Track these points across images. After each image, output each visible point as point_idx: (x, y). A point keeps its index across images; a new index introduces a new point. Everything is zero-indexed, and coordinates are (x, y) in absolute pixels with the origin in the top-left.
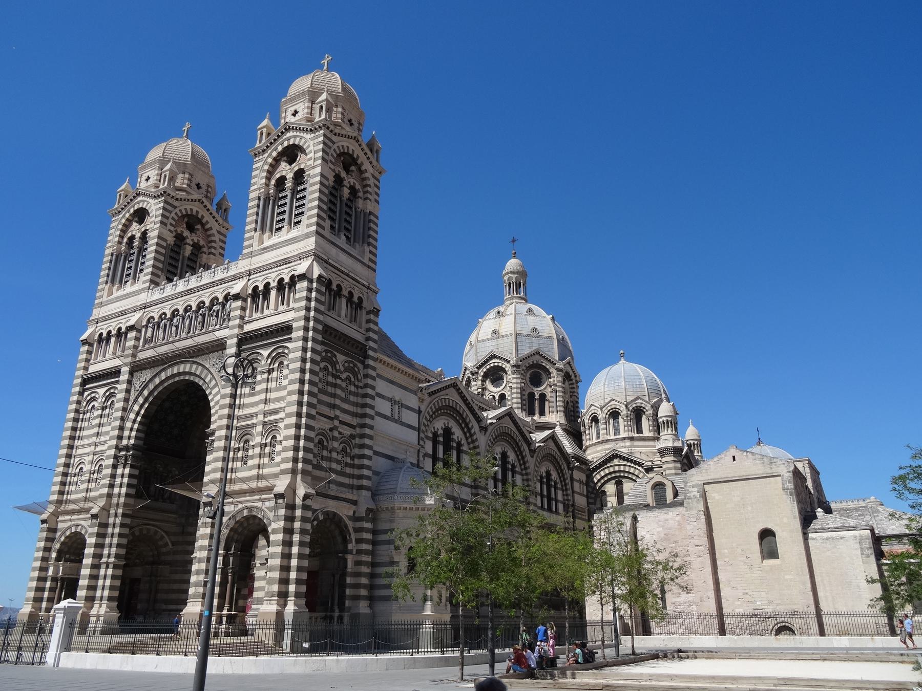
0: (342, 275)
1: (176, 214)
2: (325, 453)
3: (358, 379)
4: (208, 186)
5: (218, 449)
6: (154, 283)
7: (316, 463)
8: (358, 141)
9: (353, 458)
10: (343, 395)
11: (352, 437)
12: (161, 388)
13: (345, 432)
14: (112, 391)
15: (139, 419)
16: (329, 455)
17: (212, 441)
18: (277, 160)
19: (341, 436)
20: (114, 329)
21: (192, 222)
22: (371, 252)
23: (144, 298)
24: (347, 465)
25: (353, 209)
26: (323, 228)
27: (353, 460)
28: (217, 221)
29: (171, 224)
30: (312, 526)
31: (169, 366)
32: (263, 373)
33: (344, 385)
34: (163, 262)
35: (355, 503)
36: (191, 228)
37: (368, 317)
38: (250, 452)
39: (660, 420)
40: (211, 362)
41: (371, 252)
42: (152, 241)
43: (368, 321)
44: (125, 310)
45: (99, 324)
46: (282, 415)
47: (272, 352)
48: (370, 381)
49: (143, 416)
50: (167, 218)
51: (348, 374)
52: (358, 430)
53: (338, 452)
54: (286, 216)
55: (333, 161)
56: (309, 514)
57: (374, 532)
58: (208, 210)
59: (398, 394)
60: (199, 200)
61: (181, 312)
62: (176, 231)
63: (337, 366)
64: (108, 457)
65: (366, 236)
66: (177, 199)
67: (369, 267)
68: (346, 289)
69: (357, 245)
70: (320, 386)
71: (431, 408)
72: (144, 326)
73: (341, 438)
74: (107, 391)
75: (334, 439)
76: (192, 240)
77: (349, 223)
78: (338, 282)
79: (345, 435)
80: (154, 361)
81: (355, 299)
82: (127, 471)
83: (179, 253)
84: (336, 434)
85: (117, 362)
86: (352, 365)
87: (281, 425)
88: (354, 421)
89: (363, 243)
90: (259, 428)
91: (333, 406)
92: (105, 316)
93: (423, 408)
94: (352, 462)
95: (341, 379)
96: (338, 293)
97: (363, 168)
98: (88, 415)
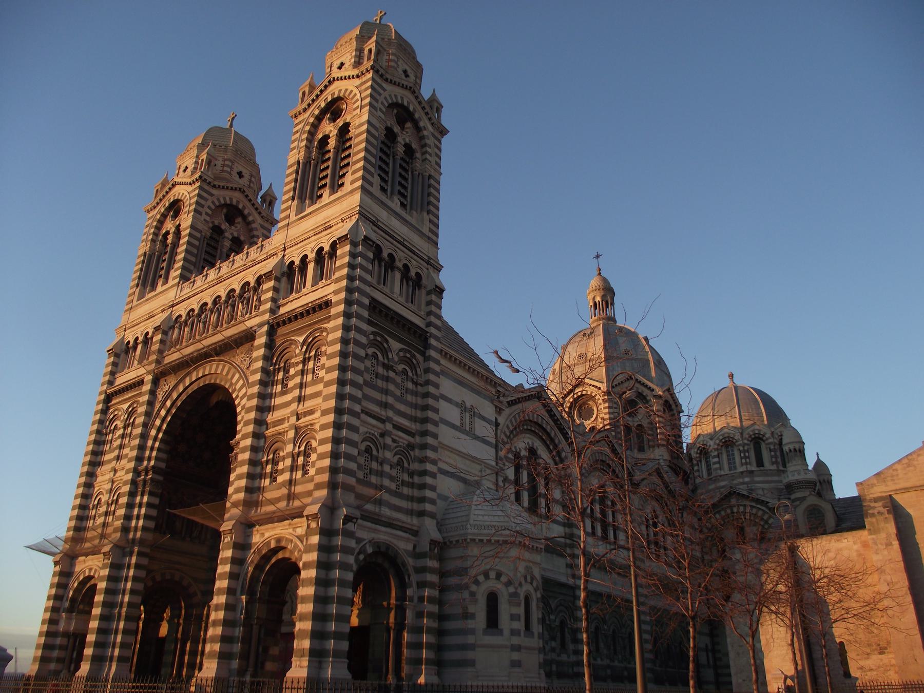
0: (395, 243)
1: (213, 202)
2: (374, 465)
3: (417, 375)
4: (251, 176)
6: (184, 278)
7: (362, 477)
8: (414, 92)
9: (411, 474)
10: (398, 393)
11: (411, 446)
13: (401, 440)
15: (160, 435)
16: (380, 468)
17: (236, 454)
18: (319, 119)
19: (395, 444)
21: (232, 213)
22: (431, 221)
23: (171, 295)
24: (403, 483)
25: (410, 173)
26: (371, 184)
27: (412, 477)
28: (260, 213)
29: (207, 214)
30: (357, 560)
31: (195, 369)
33: (398, 380)
34: (196, 256)
35: (415, 533)
36: (230, 220)
37: (429, 298)
39: (786, 448)
40: (239, 357)
41: (431, 221)
42: (185, 233)
43: (429, 303)
46: (318, 414)
47: (308, 337)
48: (432, 377)
49: (165, 432)
50: (203, 206)
51: (403, 366)
52: (418, 439)
53: (391, 466)
54: (328, 180)
55: (384, 110)
56: (352, 543)
57: (443, 574)
58: (250, 200)
59: (470, 399)
60: (240, 189)
61: (210, 305)
62: (213, 222)
63: (390, 354)
64: (125, 483)
65: (426, 203)
66: (214, 186)
67: (429, 238)
68: (400, 260)
69: (414, 213)
70: (368, 377)
71: (511, 421)
73: (396, 447)
74: (129, 407)
75: (386, 447)
76: (232, 234)
77: (405, 188)
78: (390, 251)
79: (400, 444)
80: (178, 365)
81: (413, 273)
82: (145, 499)
83: (216, 249)
84: (388, 441)
86: (408, 355)
87: (317, 427)
88: (413, 427)
89: (422, 210)
90: (291, 434)
91: (385, 405)
93: (501, 420)
94: (411, 480)
95: (394, 371)
96: (390, 264)
97: (421, 124)
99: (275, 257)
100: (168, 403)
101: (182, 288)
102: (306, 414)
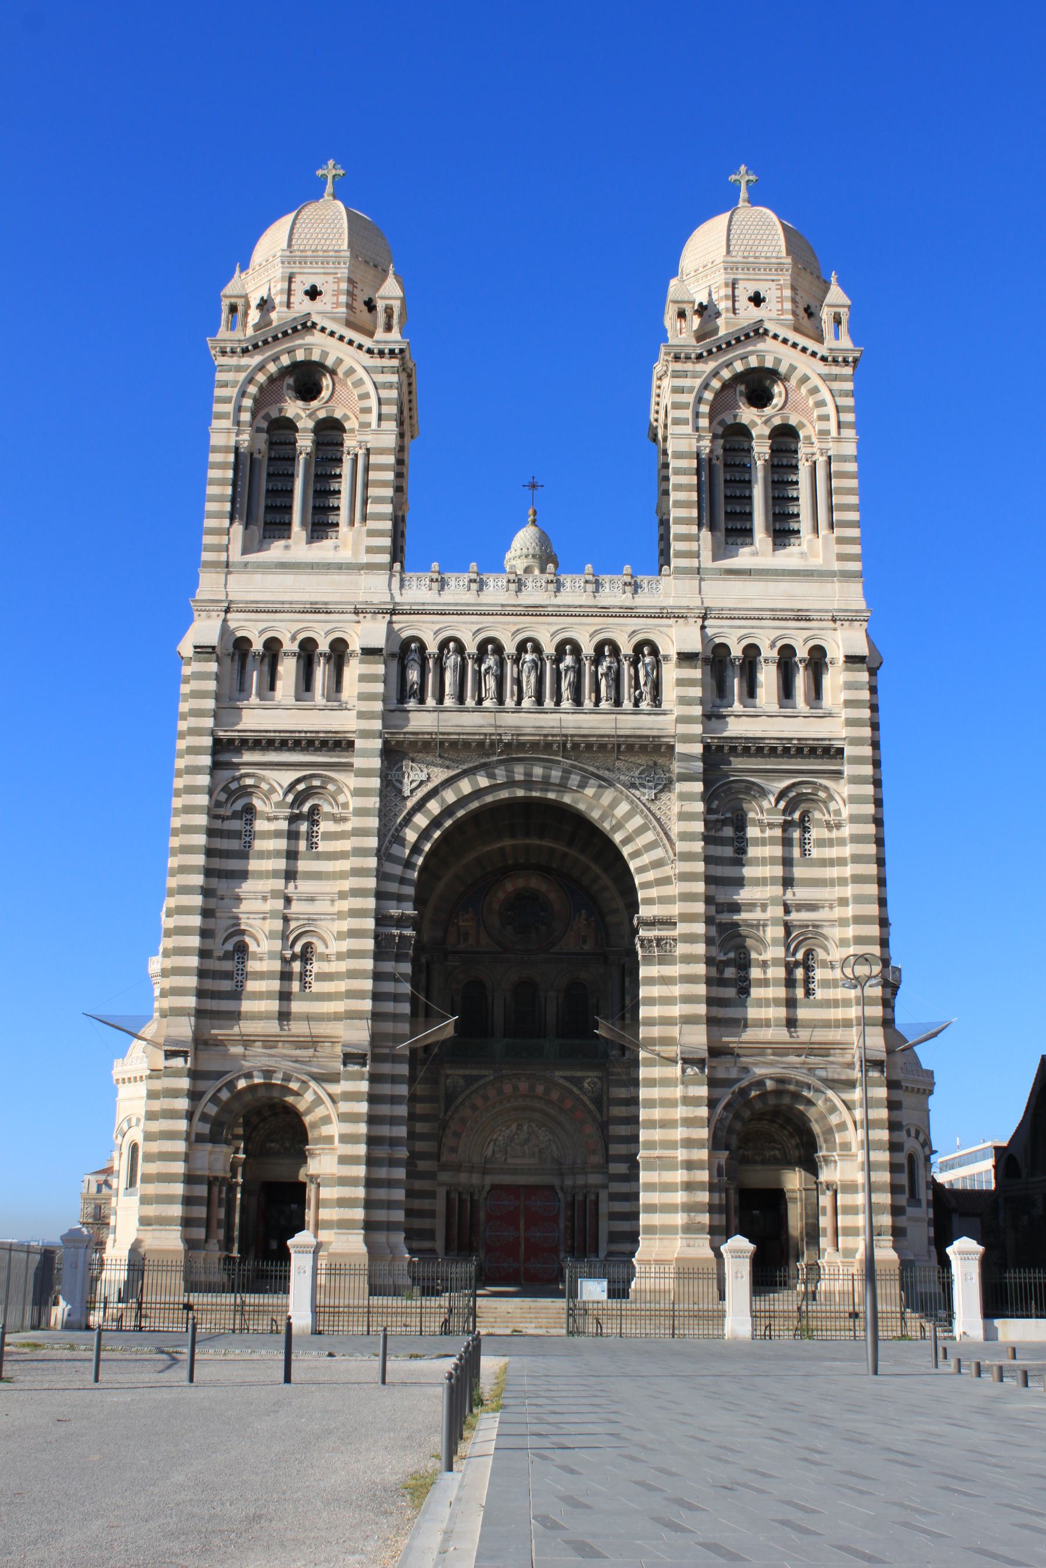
12: (475, 805)
14: (316, 783)
44: (326, 603)
72: (393, 655)
74: (298, 781)
80: (454, 744)
85: (344, 722)
100: (434, 807)
101: (402, 580)
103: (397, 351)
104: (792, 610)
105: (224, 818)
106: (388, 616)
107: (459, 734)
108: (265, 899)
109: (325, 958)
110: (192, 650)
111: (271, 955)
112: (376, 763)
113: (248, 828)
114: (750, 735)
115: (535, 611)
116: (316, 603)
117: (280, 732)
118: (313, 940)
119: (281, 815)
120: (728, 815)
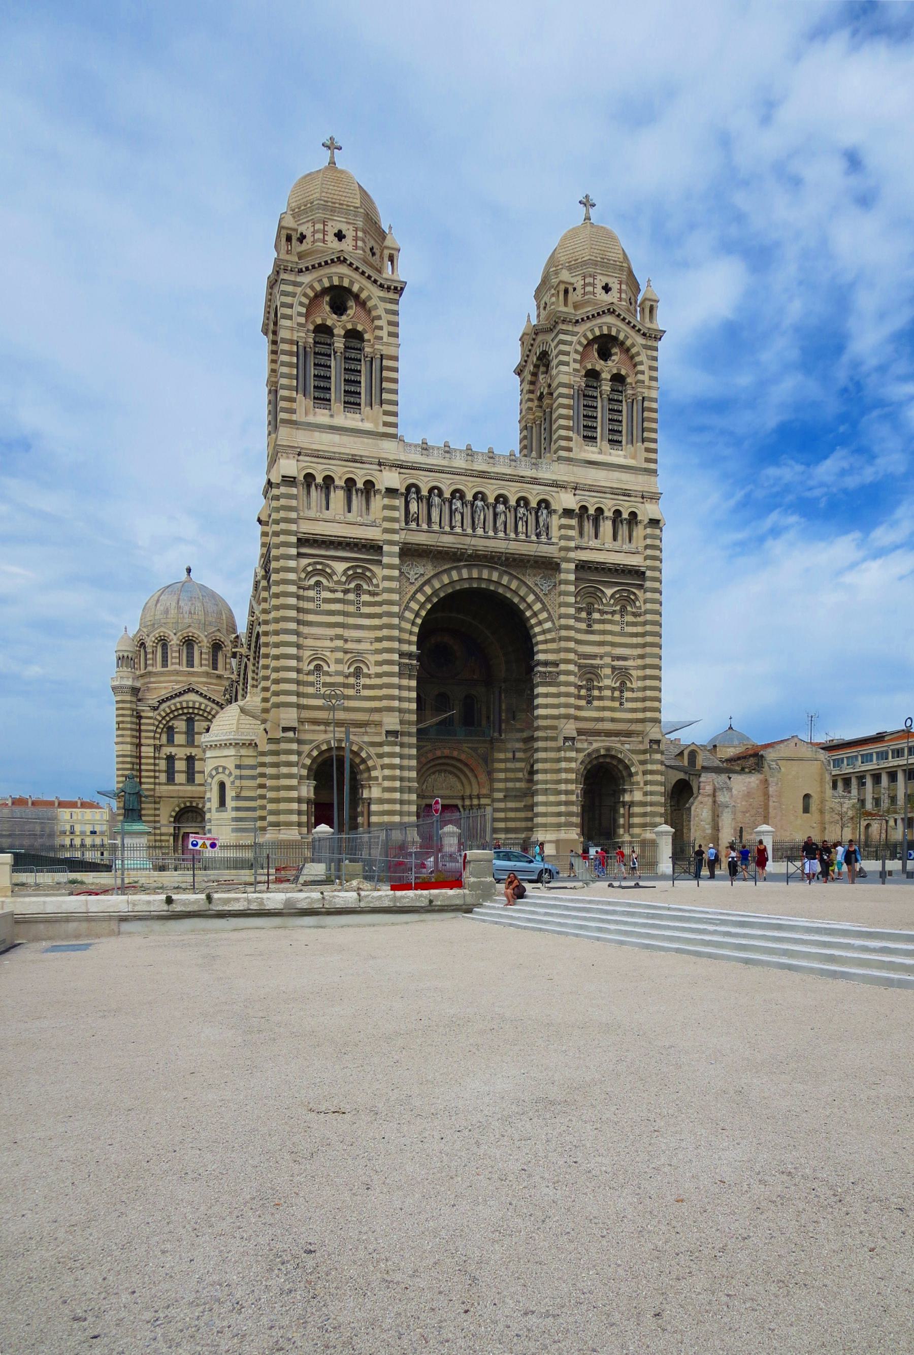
5: (567, 684)
14: (359, 571)
20: (340, 478)
32: (607, 613)
38: (596, 693)
44: (361, 456)
45: (301, 458)
47: (615, 592)
74: (349, 569)
80: (440, 552)
87: (634, 673)
90: (608, 671)
92: (319, 451)
98: (311, 593)
99: (563, 489)
102: (619, 658)
103: (399, 289)
104: (622, 489)
105: (304, 589)
106: (398, 469)
107: (443, 547)
108: (331, 639)
109: (369, 676)
110: (281, 478)
111: (338, 673)
112: (396, 561)
113: (318, 596)
114: (597, 560)
115: (483, 475)
116: (356, 455)
117: (338, 537)
118: (361, 665)
119: (340, 589)
120: (584, 605)
